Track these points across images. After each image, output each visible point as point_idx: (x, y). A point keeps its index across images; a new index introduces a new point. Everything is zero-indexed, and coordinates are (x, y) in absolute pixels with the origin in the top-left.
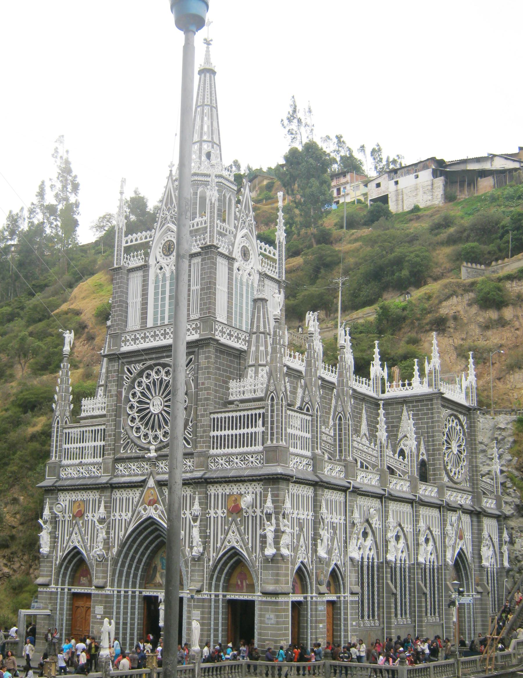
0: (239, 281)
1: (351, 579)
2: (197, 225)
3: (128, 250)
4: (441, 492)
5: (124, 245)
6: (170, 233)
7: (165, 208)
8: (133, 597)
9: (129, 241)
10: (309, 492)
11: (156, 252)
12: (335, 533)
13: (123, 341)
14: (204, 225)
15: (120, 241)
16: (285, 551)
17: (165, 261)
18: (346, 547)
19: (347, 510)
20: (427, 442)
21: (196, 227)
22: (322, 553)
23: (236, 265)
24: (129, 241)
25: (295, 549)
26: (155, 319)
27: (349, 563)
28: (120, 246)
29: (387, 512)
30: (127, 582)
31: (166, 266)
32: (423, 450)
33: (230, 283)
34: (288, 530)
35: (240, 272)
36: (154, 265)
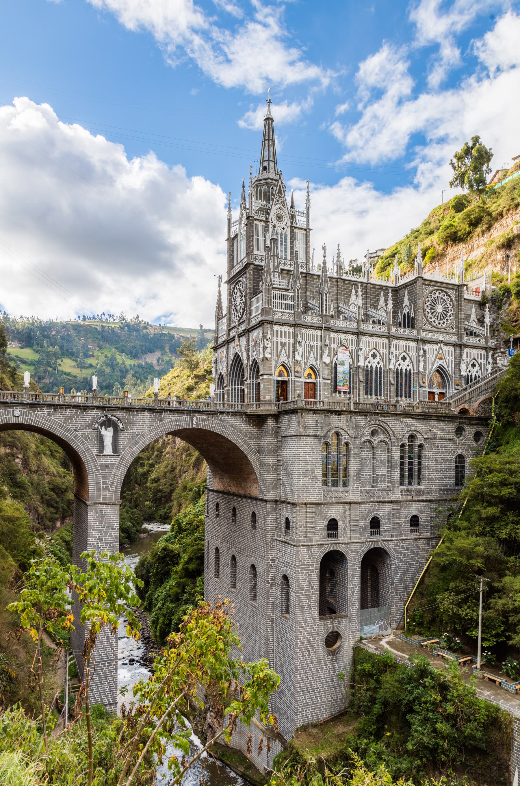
1: (326, 372)
4: (418, 333)
8: (238, 390)
10: (292, 330)
12: (312, 350)
16: (268, 356)
18: (321, 357)
19: (322, 339)
20: (414, 306)
22: (298, 358)
25: (278, 356)
27: (322, 364)
29: (359, 341)
30: (235, 383)
32: (413, 312)
34: (269, 346)
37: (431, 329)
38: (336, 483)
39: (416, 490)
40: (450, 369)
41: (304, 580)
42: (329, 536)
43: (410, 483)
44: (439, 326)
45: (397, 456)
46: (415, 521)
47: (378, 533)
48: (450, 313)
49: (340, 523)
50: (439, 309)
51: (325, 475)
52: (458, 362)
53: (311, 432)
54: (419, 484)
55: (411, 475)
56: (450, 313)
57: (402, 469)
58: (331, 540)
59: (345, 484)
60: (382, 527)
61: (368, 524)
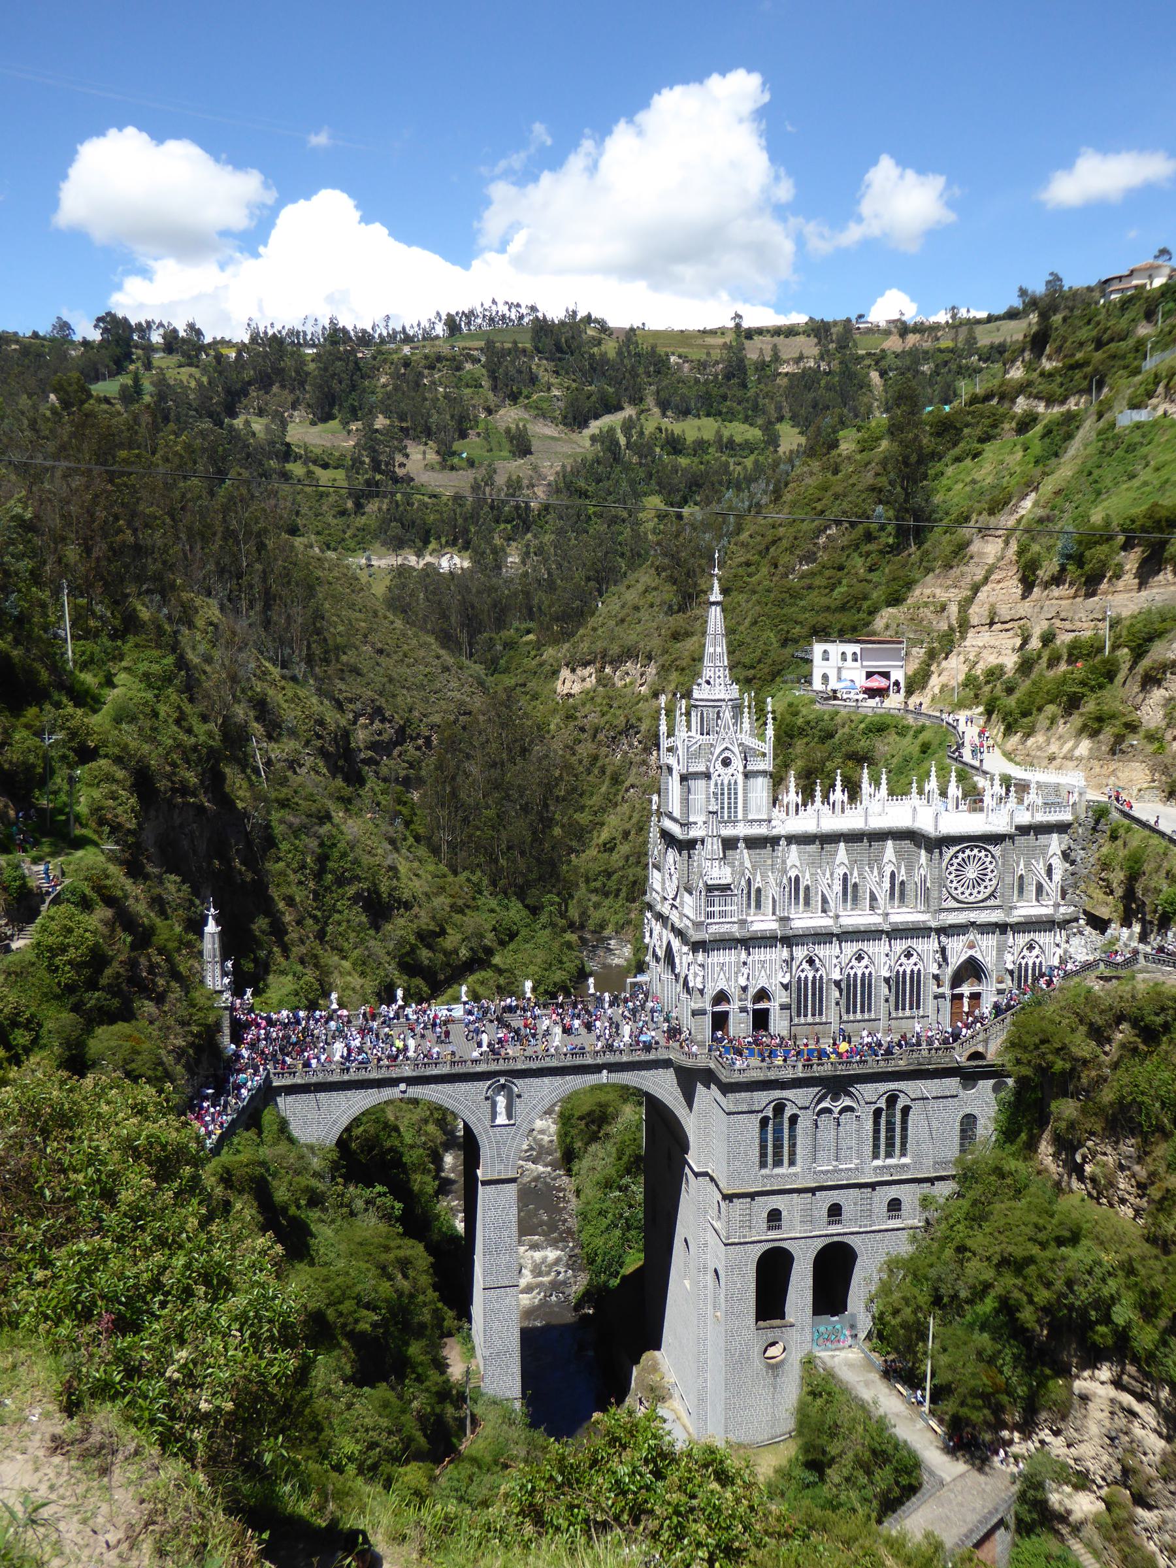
37: (957, 905)
38: (778, 1163)
39: (897, 1166)
40: (988, 959)
41: (735, 1283)
42: (769, 1228)
43: (889, 1155)
44: (971, 899)
45: (869, 1125)
46: (895, 1206)
47: (839, 1222)
48: (991, 875)
49: (784, 1214)
50: (971, 873)
51: (763, 1155)
52: (1001, 950)
53: (745, 1108)
54: (903, 1154)
55: (890, 1145)
56: (991, 875)
57: (876, 1138)
58: (773, 1235)
59: (792, 1163)
60: (844, 1217)
61: (825, 1212)
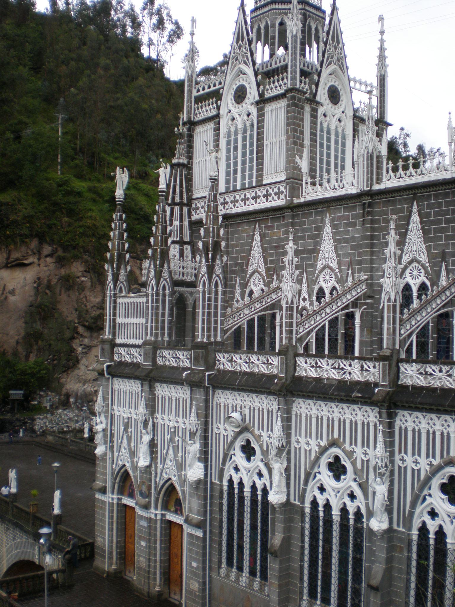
0: (325, 129)
2: (276, 63)
3: (199, 100)
5: (195, 93)
6: (241, 75)
7: (236, 45)
9: (201, 89)
11: (228, 99)
13: (194, 209)
14: (283, 63)
15: (190, 91)
17: (237, 110)
21: (274, 66)
23: (321, 111)
24: (201, 89)
26: (228, 182)
28: (190, 96)
31: (238, 117)
33: (313, 134)
35: (328, 118)
36: (225, 115)
